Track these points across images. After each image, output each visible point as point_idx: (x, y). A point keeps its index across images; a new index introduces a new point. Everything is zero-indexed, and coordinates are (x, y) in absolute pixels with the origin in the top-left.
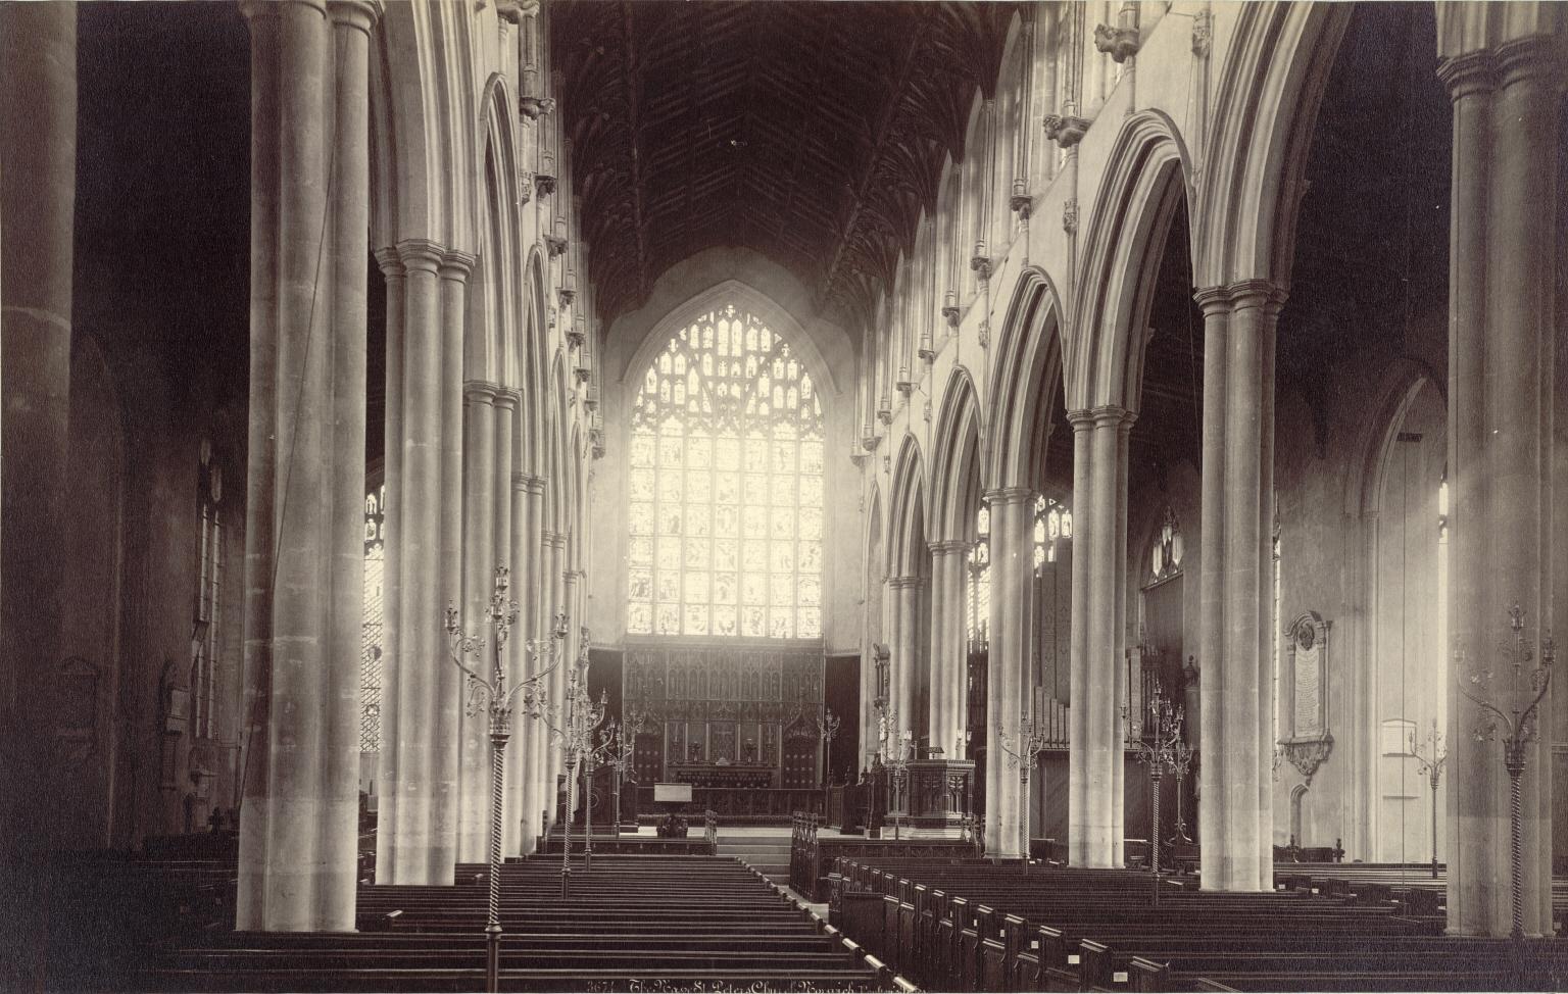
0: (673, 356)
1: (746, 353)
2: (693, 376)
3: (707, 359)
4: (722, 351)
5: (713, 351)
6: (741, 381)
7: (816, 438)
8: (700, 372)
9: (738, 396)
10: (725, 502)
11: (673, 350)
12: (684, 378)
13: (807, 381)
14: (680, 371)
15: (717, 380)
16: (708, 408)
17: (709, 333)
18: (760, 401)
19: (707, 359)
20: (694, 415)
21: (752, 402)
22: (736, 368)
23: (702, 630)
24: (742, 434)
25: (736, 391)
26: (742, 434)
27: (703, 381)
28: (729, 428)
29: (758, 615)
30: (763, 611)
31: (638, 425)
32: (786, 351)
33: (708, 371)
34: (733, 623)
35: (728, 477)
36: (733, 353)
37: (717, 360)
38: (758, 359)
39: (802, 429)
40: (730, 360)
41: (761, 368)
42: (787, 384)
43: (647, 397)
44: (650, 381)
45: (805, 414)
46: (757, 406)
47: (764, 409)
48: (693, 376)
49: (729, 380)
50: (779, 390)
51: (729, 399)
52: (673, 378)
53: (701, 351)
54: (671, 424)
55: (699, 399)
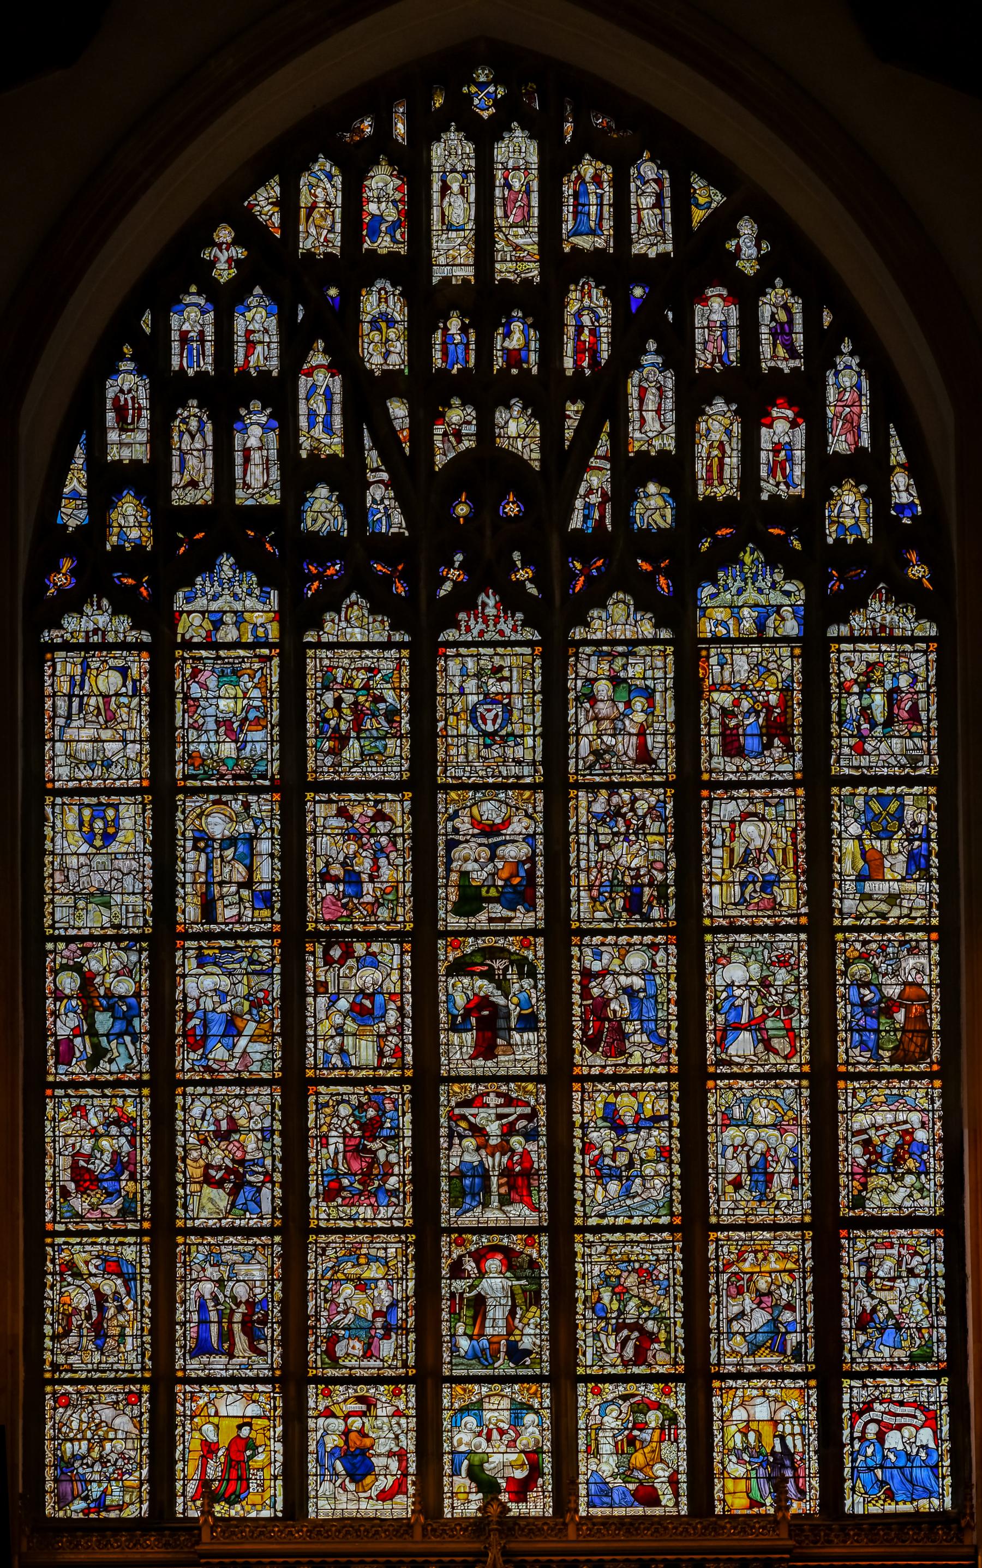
0: (225, 302)
1: (561, 267)
2: (319, 386)
3: (380, 302)
4: (452, 258)
5: (411, 270)
6: (543, 394)
7: (903, 621)
8: (346, 362)
9: (532, 454)
10: (481, 920)
11: (224, 273)
12: (279, 394)
13: (846, 383)
14: (265, 357)
15: (428, 389)
16: (386, 513)
17: (382, 181)
18: (632, 472)
19: (380, 302)
20: (326, 547)
21: (597, 479)
22: (517, 336)
23: (385, 1496)
24: (555, 627)
25: (517, 428)
26: (555, 627)
27: (363, 396)
28: (490, 601)
29: (653, 1418)
30: (677, 1401)
31: (73, 602)
32: (747, 245)
33: (384, 351)
34: (533, 1456)
35: (490, 811)
36: (504, 270)
37: (428, 304)
38: (617, 296)
39: (835, 585)
40: (487, 302)
41: (630, 333)
42: (752, 392)
43: (108, 482)
44: (121, 411)
45: (849, 507)
46: (622, 496)
47: (654, 507)
48: (319, 386)
49: (485, 390)
50: (718, 423)
51: (488, 467)
52: (226, 394)
53: (356, 267)
54: (229, 604)
55: (346, 478)
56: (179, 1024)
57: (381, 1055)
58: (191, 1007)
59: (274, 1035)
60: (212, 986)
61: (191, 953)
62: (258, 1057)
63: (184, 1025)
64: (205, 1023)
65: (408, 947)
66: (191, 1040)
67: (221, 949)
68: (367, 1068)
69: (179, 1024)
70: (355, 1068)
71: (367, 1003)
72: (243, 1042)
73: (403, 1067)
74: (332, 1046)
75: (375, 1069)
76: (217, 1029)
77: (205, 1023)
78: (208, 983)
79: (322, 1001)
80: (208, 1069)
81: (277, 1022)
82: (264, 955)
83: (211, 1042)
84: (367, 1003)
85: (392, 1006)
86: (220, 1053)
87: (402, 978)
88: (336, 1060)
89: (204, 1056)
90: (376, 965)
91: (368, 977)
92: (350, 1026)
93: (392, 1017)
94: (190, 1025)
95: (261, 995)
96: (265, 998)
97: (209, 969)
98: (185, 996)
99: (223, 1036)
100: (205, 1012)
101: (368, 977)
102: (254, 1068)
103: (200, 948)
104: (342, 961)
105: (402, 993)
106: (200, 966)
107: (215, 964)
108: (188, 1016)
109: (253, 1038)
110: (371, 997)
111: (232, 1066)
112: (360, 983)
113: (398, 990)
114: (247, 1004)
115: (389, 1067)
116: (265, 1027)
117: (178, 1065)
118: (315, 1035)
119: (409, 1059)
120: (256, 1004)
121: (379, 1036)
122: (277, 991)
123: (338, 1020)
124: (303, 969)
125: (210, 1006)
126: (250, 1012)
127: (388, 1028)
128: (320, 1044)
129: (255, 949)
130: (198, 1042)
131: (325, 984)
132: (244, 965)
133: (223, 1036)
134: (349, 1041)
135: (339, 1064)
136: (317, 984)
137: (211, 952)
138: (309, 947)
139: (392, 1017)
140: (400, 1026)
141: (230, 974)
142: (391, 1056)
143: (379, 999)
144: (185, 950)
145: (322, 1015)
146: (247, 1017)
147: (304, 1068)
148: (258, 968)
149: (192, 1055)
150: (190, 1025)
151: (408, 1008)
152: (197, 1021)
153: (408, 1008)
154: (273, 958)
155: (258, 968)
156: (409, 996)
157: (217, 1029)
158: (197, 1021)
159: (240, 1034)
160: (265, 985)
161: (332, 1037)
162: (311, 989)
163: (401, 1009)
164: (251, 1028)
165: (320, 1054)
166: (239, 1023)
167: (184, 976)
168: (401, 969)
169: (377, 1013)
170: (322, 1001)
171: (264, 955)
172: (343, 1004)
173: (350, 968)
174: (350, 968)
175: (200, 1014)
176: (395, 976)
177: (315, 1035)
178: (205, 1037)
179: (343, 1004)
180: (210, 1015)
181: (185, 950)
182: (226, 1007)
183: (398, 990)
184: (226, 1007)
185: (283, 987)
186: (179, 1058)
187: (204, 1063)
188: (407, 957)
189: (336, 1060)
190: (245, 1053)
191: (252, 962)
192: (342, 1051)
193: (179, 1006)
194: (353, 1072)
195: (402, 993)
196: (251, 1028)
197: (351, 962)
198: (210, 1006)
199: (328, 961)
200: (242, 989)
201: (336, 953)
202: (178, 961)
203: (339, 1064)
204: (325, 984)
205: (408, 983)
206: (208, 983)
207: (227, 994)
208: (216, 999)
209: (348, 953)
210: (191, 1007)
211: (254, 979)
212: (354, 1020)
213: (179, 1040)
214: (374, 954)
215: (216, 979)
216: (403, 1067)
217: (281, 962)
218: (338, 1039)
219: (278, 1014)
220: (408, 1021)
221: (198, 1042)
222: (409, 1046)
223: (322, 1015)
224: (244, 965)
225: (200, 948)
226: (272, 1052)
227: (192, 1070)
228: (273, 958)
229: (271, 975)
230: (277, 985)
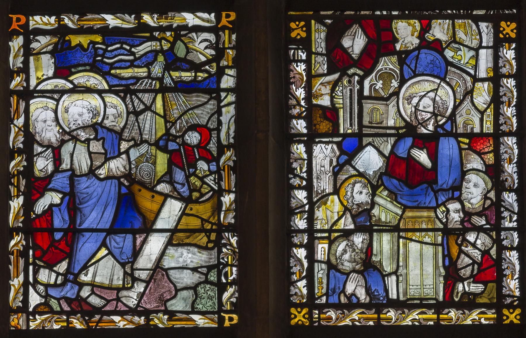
56: (16, 204)
57: (452, 275)
58: (43, 164)
59: (221, 229)
60: (87, 118)
61: (42, 42)
62: (187, 278)
63: (28, 206)
64: (73, 203)
65: (509, 29)
66: (43, 241)
67: (108, 33)
68: (421, 304)
69: (16, 204)
70: (397, 305)
71: (422, 157)
72: (155, 244)
73: (499, 304)
74: (346, 253)
75: (438, 307)
76: (97, 215)
77: (73, 203)
78: (78, 109)
79: (324, 154)
80: (79, 306)
81: (228, 199)
82: (201, 47)
83: (86, 246)
84: (422, 157)
85: (475, 162)
86: (105, 270)
87: (496, 101)
88: (354, 286)
89: (71, 277)
90: (442, 71)
91: (424, 97)
92: (386, 210)
93: (475, 189)
94: (41, 206)
95: (193, 138)
96: (202, 146)
97: (82, 78)
98: (30, 138)
99: (111, 231)
100: (73, 175)
101: (424, 97)
102: (178, 305)
103: (61, 31)
104: (368, 61)
105: (497, 135)
106: (62, 72)
107: (94, 67)
108: (37, 187)
109: (176, 237)
110: (430, 143)
111: (131, 298)
112: (407, 110)
113: (489, 127)
114: (162, 159)
115: (469, 303)
116: (204, 210)
117: (14, 298)
118: (311, 230)
119: (513, 285)
120: (182, 158)
121: (447, 231)
122: (227, 131)
123: (360, 195)
124: (285, 82)
125: (82, 162)
126: (168, 177)
127: (467, 214)
128: (321, 249)
129: (181, 32)
130: (54, 243)
131: (331, 114)
132: (157, 70)
133: (111, 231)
134: (384, 243)
135: (362, 294)
136: (312, 112)
137: (84, 40)
138: (297, 31)
139: (475, 189)
140: (494, 209)
141: (125, 90)
142: (476, 279)
143: (447, 147)
144: (30, 35)
145: (324, 184)
146: (163, 187)
147: (286, 303)
148: (187, 76)
149: (44, 275)
150: (41, 206)
151: (510, 169)
152: (54, 198)
153: (510, 169)
154: (220, 53)
155: (187, 76)
156: (511, 141)
157: (97, 215)
158: (54, 198)
159: (148, 229)
160: (202, 116)
161: (347, 234)
162: (301, 126)
163: (494, 171)
164: (171, 212)
165: (320, 272)
166: (146, 202)
167: (27, 94)
168: (496, 79)
169: (445, 178)
170: (324, 154)
171: (201, 47)
172: (370, 160)
173: (386, 77)
174: (386, 77)
175: (61, 181)
176: (482, 95)
177: (311, 230)
178: (73, 233)
179: (370, 160)
180: (83, 184)
181: (30, 35)
182: (117, 165)
183: (489, 127)
184: (117, 165)
185: (239, 118)
186: (16, 282)
187: (70, 291)
188: (510, 54)
189: (354, 286)
190: (158, 267)
191: (173, 62)
192: (368, 266)
193: (16, 164)
194: (392, 314)
195: (497, 135)
196: (171, 212)
197: (387, 64)
198: (82, 162)
199: (339, 60)
200: (152, 125)
201: (356, 43)
202: (15, 61)
203: (362, 294)
204: (331, 114)
205: (509, 111)
206: (78, 109)
207: (119, 135)
208: (96, 147)
209: (381, 42)
210: (43, 164)
211: (179, 102)
212: (394, 196)
213: (16, 242)
214: (437, 46)
215: (95, 101)
216: (499, 304)
217: (236, 63)
218: (358, 239)
219: (230, 180)
220: (510, 198)
221: (54, 243)
222: (513, 256)
223: (324, 184)
224: (157, 70)
225: (61, 31)
226: (218, 267)
227: (44, 308)
228: (220, 53)
229: (214, 91)
230: (229, 113)
